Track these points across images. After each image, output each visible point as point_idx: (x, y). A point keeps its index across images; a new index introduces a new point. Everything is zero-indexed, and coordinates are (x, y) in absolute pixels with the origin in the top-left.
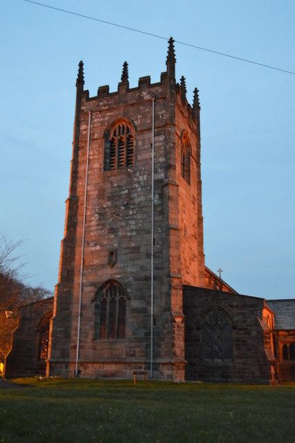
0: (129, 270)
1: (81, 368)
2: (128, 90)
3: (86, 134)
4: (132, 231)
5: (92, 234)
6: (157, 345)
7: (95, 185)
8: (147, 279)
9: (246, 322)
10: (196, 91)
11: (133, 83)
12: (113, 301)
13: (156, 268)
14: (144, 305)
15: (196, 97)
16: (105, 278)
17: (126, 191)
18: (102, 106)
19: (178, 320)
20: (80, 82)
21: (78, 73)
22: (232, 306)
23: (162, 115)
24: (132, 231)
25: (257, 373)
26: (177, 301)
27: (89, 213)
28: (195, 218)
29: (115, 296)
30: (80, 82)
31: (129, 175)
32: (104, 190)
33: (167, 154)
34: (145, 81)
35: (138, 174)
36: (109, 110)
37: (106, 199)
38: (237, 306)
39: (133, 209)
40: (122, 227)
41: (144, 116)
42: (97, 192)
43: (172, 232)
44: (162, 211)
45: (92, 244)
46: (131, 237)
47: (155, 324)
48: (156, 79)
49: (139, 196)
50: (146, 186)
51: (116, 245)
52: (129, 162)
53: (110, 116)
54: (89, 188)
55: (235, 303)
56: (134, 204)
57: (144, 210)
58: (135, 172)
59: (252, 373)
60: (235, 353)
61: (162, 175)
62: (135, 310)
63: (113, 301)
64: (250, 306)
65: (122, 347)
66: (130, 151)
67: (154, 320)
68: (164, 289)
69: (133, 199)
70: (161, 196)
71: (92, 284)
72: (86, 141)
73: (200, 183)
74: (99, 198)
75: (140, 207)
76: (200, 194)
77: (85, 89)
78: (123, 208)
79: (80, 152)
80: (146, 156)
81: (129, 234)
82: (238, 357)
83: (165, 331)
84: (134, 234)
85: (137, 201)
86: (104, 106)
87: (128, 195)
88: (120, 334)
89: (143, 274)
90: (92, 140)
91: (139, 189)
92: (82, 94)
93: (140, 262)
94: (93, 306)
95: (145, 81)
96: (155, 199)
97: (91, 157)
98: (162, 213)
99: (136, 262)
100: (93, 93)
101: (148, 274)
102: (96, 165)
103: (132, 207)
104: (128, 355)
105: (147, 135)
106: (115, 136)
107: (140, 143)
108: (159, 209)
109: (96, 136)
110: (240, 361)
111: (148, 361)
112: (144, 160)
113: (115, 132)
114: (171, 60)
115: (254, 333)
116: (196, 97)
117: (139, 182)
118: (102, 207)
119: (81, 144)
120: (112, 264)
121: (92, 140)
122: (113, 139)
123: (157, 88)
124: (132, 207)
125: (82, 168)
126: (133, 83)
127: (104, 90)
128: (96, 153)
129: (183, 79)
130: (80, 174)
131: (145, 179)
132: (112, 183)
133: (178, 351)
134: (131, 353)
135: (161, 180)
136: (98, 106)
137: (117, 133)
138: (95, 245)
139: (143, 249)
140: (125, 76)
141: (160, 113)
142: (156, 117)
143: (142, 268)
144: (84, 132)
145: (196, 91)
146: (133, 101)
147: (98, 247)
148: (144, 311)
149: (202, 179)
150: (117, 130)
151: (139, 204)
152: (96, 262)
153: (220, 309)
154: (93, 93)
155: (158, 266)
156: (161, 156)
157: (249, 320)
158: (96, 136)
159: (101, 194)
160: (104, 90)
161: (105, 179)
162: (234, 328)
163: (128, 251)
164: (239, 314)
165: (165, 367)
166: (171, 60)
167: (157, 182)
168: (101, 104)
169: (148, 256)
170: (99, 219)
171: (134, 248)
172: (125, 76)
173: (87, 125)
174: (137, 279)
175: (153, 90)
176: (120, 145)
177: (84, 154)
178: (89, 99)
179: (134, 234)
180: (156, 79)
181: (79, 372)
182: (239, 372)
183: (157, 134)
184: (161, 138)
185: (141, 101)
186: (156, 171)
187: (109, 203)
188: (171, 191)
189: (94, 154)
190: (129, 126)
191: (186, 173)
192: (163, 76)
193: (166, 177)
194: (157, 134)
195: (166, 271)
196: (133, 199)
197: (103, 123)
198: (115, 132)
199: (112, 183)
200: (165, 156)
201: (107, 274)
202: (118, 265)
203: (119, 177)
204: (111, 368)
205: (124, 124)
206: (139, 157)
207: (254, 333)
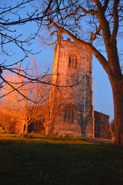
1: (59, 132)
4: (78, 89)
6: (85, 126)
9: (105, 122)
13: (86, 103)
14: (82, 114)
17: (77, 76)
18: (69, 45)
19: (94, 120)
22: (101, 117)
24: (78, 89)
25: (107, 136)
31: (78, 71)
32: (69, 73)
35: (80, 72)
36: (71, 47)
38: (103, 117)
41: (83, 54)
42: (66, 73)
47: (85, 120)
53: (72, 49)
55: (102, 116)
58: (79, 71)
60: (102, 130)
65: (73, 126)
66: (76, 63)
68: (89, 110)
69: (78, 79)
70: (88, 81)
72: (62, 55)
74: (67, 76)
78: (75, 81)
79: (60, 58)
80: (83, 67)
81: (77, 90)
82: (102, 131)
83: (89, 123)
86: (70, 45)
89: (81, 104)
91: (81, 77)
96: (86, 81)
97: (64, 61)
98: (88, 86)
101: (83, 104)
104: (75, 128)
105: (84, 60)
106: (72, 56)
107: (81, 62)
108: (87, 85)
109: (66, 54)
110: (103, 132)
112: (82, 68)
113: (72, 55)
115: (107, 125)
117: (81, 74)
118: (68, 79)
119: (60, 55)
125: (60, 63)
128: (66, 60)
134: (77, 128)
135: (88, 76)
137: (72, 56)
139: (82, 96)
142: (87, 55)
144: (62, 51)
148: (81, 115)
155: (87, 102)
156: (88, 68)
157: (105, 121)
158: (66, 54)
159: (68, 75)
161: (69, 70)
162: (102, 123)
164: (103, 119)
165: (88, 133)
168: (68, 44)
169: (83, 98)
173: (63, 49)
174: (79, 105)
176: (73, 60)
177: (61, 59)
179: (79, 90)
181: (58, 133)
183: (87, 61)
184: (88, 63)
186: (86, 72)
187: (70, 78)
189: (65, 60)
190: (77, 55)
194: (87, 61)
195: (90, 104)
198: (72, 55)
200: (90, 69)
203: (74, 71)
204: (69, 132)
205: (75, 54)
206: (81, 66)
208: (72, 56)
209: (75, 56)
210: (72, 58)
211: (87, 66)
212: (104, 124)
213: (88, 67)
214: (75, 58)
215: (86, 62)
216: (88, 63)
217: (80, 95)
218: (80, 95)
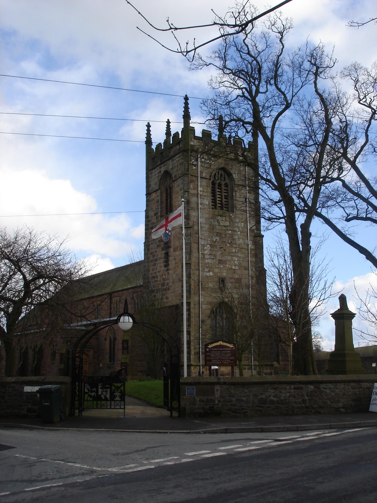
7: (206, 219)
37: (215, 234)
39: (235, 248)
40: (229, 260)
45: (206, 270)
46: (234, 270)
49: (239, 239)
51: (224, 274)
56: (236, 244)
57: (243, 251)
58: (235, 217)
78: (228, 245)
84: (237, 268)
103: (234, 246)
111: (250, 364)
117: (239, 228)
124: (234, 246)
131: (243, 226)
138: (209, 271)
147: (211, 274)
159: (212, 228)
161: (214, 217)
163: (233, 281)
170: (211, 250)
171: (238, 279)
187: (218, 238)
189: (203, 191)
214: (223, 183)
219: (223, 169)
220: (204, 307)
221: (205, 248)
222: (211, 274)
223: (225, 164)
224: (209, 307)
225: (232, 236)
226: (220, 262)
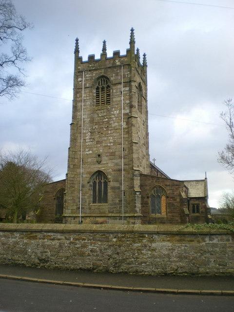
0: (109, 165)
2: (107, 59)
3: (82, 84)
4: (110, 143)
5: (87, 144)
8: (120, 170)
9: (174, 194)
10: (144, 55)
11: (110, 54)
12: (100, 183)
13: (125, 165)
14: (118, 185)
15: (144, 58)
16: (96, 170)
20: (77, 51)
21: (75, 48)
22: (166, 185)
23: (128, 74)
24: (110, 143)
25: (180, 221)
26: (137, 182)
27: (86, 130)
28: (144, 133)
29: (101, 179)
30: (77, 51)
33: (131, 98)
34: (116, 54)
35: (114, 109)
36: (95, 70)
38: (169, 185)
40: (105, 140)
41: (117, 75)
43: (134, 144)
44: (128, 132)
47: (124, 195)
48: (123, 53)
50: (119, 116)
52: (108, 102)
54: (84, 115)
55: (168, 184)
57: (118, 131)
59: (177, 221)
61: (128, 111)
62: (113, 188)
63: (100, 183)
64: (177, 185)
66: (109, 95)
67: (124, 193)
69: (111, 124)
70: (127, 123)
71: (89, 173)
73: (147, 112)
75: (115, 129)
76: (147, 119)
77: (79, 56)
80: (119, 99)
84: (112, 144)
85: (113, 125)
87: (108, 122)
88: (105, 200)
89: (118, 167)
90: (86, 88)
91: (114, 119)
92: (78, 59)
93: (115, 161)
94: (89, 185)
95: (116, 54)
96: (124, 125)
99: (113, 161)
100: (85, 59)
102: (88, 103)
105: (119, 86)
107: (114, 91)
109: (88, 85)
110: (170, 214)
111: (121, 215)
114: (132, 42)
116: (144, 58)
117: (114, 115)
120: (99, 162)
121: (86, 88)
122: (98, 87)
123: (124, 58)
124: (110, 129)
126: (110, 54)
127: (91, 58)
129: (138, 50)
130: (78, 108)
132: (98, 114)
133: (138, 209)
135: (127, 114)
136: (89, 67)
137: (100, 84)
138: (89, 151)
139: (117, 153)
140: (104, 49)
141: (126, 73)
142: (124, 76)
143: (117, 164)
144: (80, 83)
145: (144, 55)
146: (111, 65)
147: (91, 152)
148: (119, 188)
149: (148, 109)
150: (100, 82)
151: (115, 127)
152: (89, 160)
153: (160, 187)
154: (85, 59)
157: (175, 193)
159: (92, 121)
160: (91, 58)
161: (94, 112)
164: (170, 189)
165: (131, 218)
166: (132, 42)
167: (125, 114)
171: (112, 152)
172: (104, 49)
173: (82, 78)
175: (122, 59)
178: (82, 63)
179: (112, 144)
180: (123, 53)
182: (170, 221)
184: (127, 89)
185: (114, 67)
187: (97, 126)
188: (134, 121)
191: (140, 106)
192: (128, 51)
193: (131, 112)
194: (125, 86)
195: (131, 166)
196: (111, 124)
197: (92, 77)
199: (98, 114)
201: (96, 168)
202: (102, 162)
206: (114, 99)
207: (178, 200)
208: (100, 84)
209: (105, 83)
210: (100, 87)
211: (125, 95)
212: (172, 198)
213: (128, 97)
214: (105, 86)
215: (123, 89)
216: (127, 89)
217: (115, 152)
218: (115, 152)
219: (103, 76)
220: (84, 176)
221: (87, 135)
222: (91, 152)
223: (104, 72)
224: (88, 176)
225: (108, 122)
226: (98, 142)
